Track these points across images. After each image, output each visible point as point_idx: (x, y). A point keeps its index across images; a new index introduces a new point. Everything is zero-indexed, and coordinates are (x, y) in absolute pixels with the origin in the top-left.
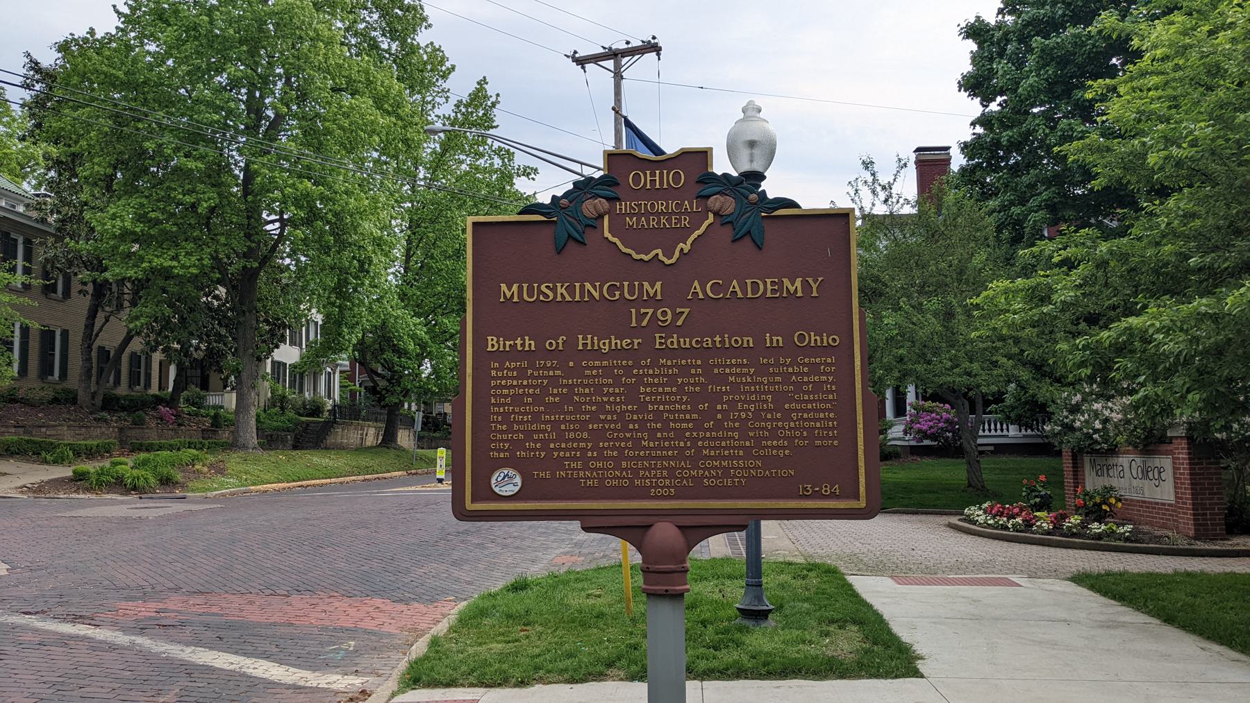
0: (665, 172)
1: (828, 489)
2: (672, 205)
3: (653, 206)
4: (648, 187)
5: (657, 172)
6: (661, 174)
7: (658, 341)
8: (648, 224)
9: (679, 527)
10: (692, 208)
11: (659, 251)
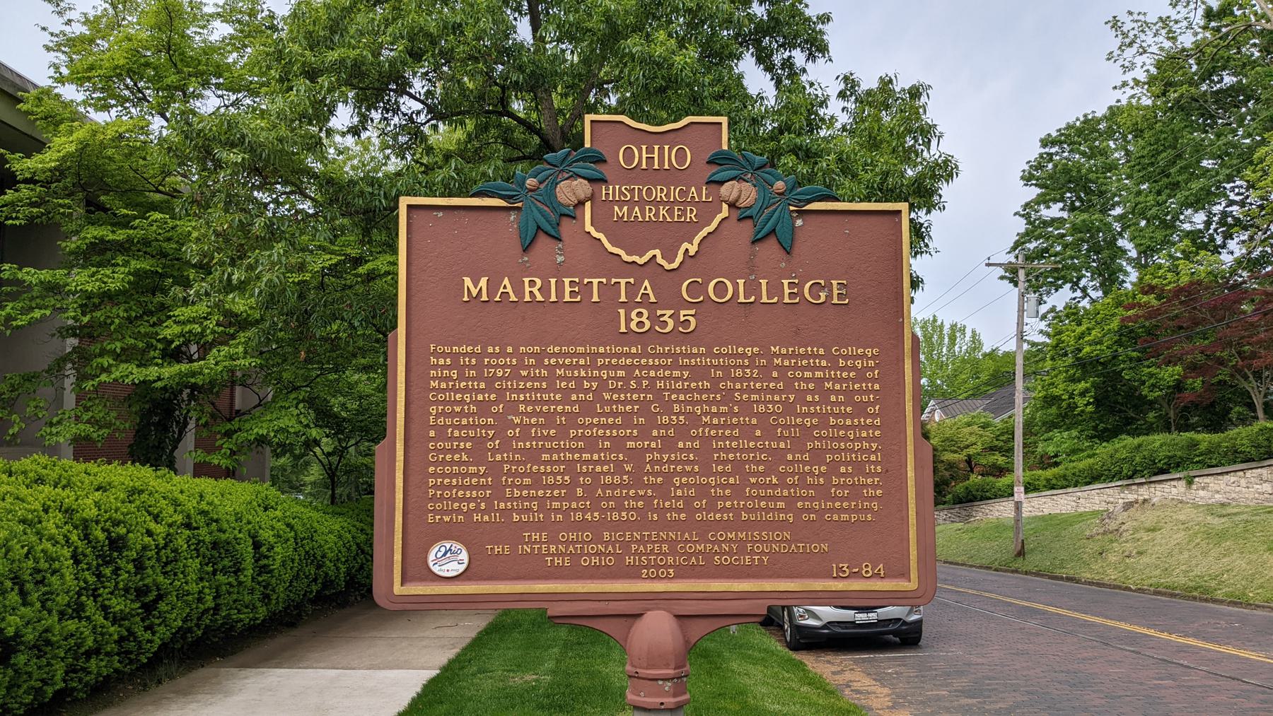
0: (666, 147)
1: (869, 569)
2: (675, 193)
3: (649, 191)
4: (644, 166)
5: (656, 147)
6: (661, 150)
7: (787, 291)
8: (643, 215)
9: (678, 617)
10: (700, 195)
11: (657, 252)
